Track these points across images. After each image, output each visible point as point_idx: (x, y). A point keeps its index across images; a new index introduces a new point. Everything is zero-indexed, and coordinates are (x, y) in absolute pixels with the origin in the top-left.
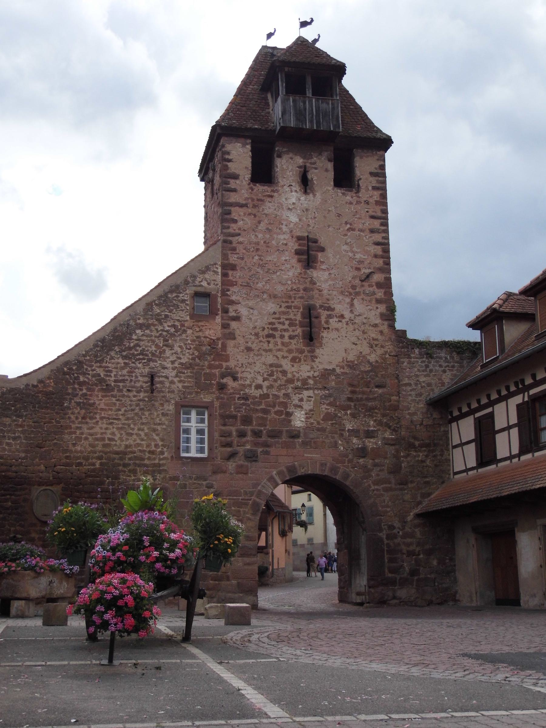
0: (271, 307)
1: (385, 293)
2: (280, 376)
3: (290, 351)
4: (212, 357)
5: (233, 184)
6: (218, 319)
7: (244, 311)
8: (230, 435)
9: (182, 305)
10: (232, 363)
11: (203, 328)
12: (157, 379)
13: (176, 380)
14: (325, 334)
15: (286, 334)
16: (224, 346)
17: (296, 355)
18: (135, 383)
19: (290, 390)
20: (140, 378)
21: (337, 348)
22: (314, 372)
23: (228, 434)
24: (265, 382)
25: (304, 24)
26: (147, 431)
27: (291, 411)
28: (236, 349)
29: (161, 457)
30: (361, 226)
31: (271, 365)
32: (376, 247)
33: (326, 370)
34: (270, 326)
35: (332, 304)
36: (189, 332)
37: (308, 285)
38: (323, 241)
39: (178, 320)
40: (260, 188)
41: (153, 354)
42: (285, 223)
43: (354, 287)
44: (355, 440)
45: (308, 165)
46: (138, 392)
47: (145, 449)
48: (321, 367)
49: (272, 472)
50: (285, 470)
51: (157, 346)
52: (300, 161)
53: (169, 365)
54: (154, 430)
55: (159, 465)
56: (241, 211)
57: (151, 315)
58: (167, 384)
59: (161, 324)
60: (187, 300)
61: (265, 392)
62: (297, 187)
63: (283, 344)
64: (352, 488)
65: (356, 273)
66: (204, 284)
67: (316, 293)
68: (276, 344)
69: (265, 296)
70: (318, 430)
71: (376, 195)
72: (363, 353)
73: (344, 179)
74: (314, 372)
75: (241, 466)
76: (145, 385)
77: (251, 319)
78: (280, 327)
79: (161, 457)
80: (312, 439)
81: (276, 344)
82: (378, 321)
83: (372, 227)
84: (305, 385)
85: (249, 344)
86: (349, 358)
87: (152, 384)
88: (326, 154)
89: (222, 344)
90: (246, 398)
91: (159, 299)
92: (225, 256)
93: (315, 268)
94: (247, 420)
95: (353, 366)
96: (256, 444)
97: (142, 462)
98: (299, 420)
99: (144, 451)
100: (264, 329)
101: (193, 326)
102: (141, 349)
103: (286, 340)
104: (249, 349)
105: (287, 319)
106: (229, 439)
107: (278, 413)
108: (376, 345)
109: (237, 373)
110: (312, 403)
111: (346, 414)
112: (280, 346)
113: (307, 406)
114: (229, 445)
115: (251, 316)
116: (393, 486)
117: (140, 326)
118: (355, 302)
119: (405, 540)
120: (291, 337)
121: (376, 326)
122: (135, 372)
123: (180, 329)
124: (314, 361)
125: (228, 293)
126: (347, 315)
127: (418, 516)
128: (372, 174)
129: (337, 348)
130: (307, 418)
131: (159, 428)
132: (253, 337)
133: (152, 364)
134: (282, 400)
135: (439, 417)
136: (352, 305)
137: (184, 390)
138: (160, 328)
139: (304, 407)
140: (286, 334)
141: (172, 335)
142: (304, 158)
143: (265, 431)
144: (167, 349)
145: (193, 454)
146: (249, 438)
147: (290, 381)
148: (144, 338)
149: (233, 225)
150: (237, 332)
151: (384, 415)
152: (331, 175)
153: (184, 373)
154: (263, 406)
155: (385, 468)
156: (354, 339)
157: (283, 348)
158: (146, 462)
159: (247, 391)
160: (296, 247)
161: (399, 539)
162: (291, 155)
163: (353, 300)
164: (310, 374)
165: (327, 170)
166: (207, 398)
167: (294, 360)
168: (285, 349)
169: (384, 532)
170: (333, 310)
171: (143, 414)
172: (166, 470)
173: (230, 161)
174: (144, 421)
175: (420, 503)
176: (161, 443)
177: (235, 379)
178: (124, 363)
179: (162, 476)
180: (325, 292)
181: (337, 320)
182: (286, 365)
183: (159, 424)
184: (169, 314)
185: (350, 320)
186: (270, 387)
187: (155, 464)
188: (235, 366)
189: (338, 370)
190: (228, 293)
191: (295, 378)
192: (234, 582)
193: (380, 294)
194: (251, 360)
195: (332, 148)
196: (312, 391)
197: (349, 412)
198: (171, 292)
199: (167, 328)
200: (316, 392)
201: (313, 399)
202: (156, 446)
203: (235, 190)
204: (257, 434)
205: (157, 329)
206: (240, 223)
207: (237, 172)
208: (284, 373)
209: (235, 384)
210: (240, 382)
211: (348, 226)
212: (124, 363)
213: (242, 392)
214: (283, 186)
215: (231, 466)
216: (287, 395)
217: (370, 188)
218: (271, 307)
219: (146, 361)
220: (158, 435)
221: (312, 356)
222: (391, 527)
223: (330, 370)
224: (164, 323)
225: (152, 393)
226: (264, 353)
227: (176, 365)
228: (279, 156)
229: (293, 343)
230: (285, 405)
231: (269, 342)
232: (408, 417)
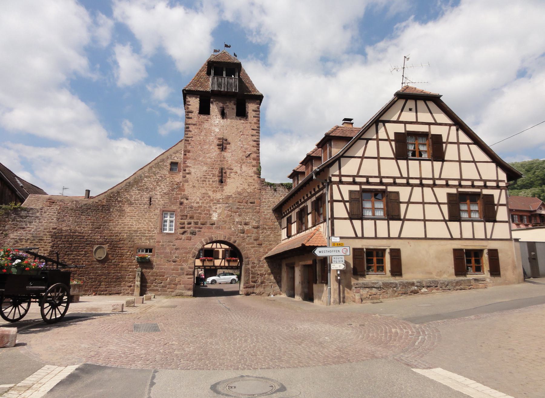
1: (257, 163)
5: (190, 115)
6: (181, 174)
7: (193, 171)
8: (184, 224)
10: (186, 193)
12: (152, 199)
13: (161, 200)
14: (228, 180)
16: (183, 185)
19: (211, 204)
25: (226, 46)
30: (247, 133)
31: (204, 194)
35: (232, 167)
36: (168, 179)
37: (222, 159)
38: (229, 140)
40: (202, 116)
41: (152, 189)
43: (242, 160)
44: (239, 226)
46: (144, 205)
48: (226, 194)
51: (153, 185)
53: (159, 193)
54: (151, 221)
55: (152, 236)
56: (194, 127)
62: (219, 116)
63: (209, 184)
65: (244, 154)
66: (176, 158)
67: (225, 163)
70: (223, 221)
71: (255, 120)
73: (242, 113)
78: (208, 177)
82: (253, 175)
83: (252, 134)
84: (218, 202)
85: (194, 184)
88: (233, 102)
92: (186, 147)
93: (225, 152)
96: (195, 228)
98: (215, 217)
103: (211, 182)
104: (194, 187)
106: (183, 226)
107: (205, 214)
112: (208, 185)
113: (219, 211)
114: (183, 228)
117: (146, 177)
118: (243, 166)
120: (213, 182)
121: (252, 176)
123: (163, 178)
126: (239, 172)
127: (266, 258)
128: (254, 111)
129: (233, 186)
131: (152, 220)
136: (241, 167)
138: (155, 177)
140: (211, 180)
145: (167, 231)
146: (192, 225)
149: (189, 133)
150: (189, 179)
151: (253, 215)
152: (235, 111)
154: (199, 211)
156: (241, 183)
158: (146, 235)
160: (218, 142)
165: (233, 109)
166: (174, 208)
167: (214, 191)
175: (267, 253)
177: (187, 199)
182: (210, 193)
186: (203, 203)
189: (233, 196)
193: (254, 163)
195: (236, 99)
198: (161, 162)
203: (191, 118)
204: (196, 223)
206: (193, 132)
207: (193, 110)
208: (209, 197)
215: (184, 237)
216: (210, 206)
218: (205, 168)
222: (253, 263)
225: (150, 205)
228: (212, 103)
230: (209, 211)
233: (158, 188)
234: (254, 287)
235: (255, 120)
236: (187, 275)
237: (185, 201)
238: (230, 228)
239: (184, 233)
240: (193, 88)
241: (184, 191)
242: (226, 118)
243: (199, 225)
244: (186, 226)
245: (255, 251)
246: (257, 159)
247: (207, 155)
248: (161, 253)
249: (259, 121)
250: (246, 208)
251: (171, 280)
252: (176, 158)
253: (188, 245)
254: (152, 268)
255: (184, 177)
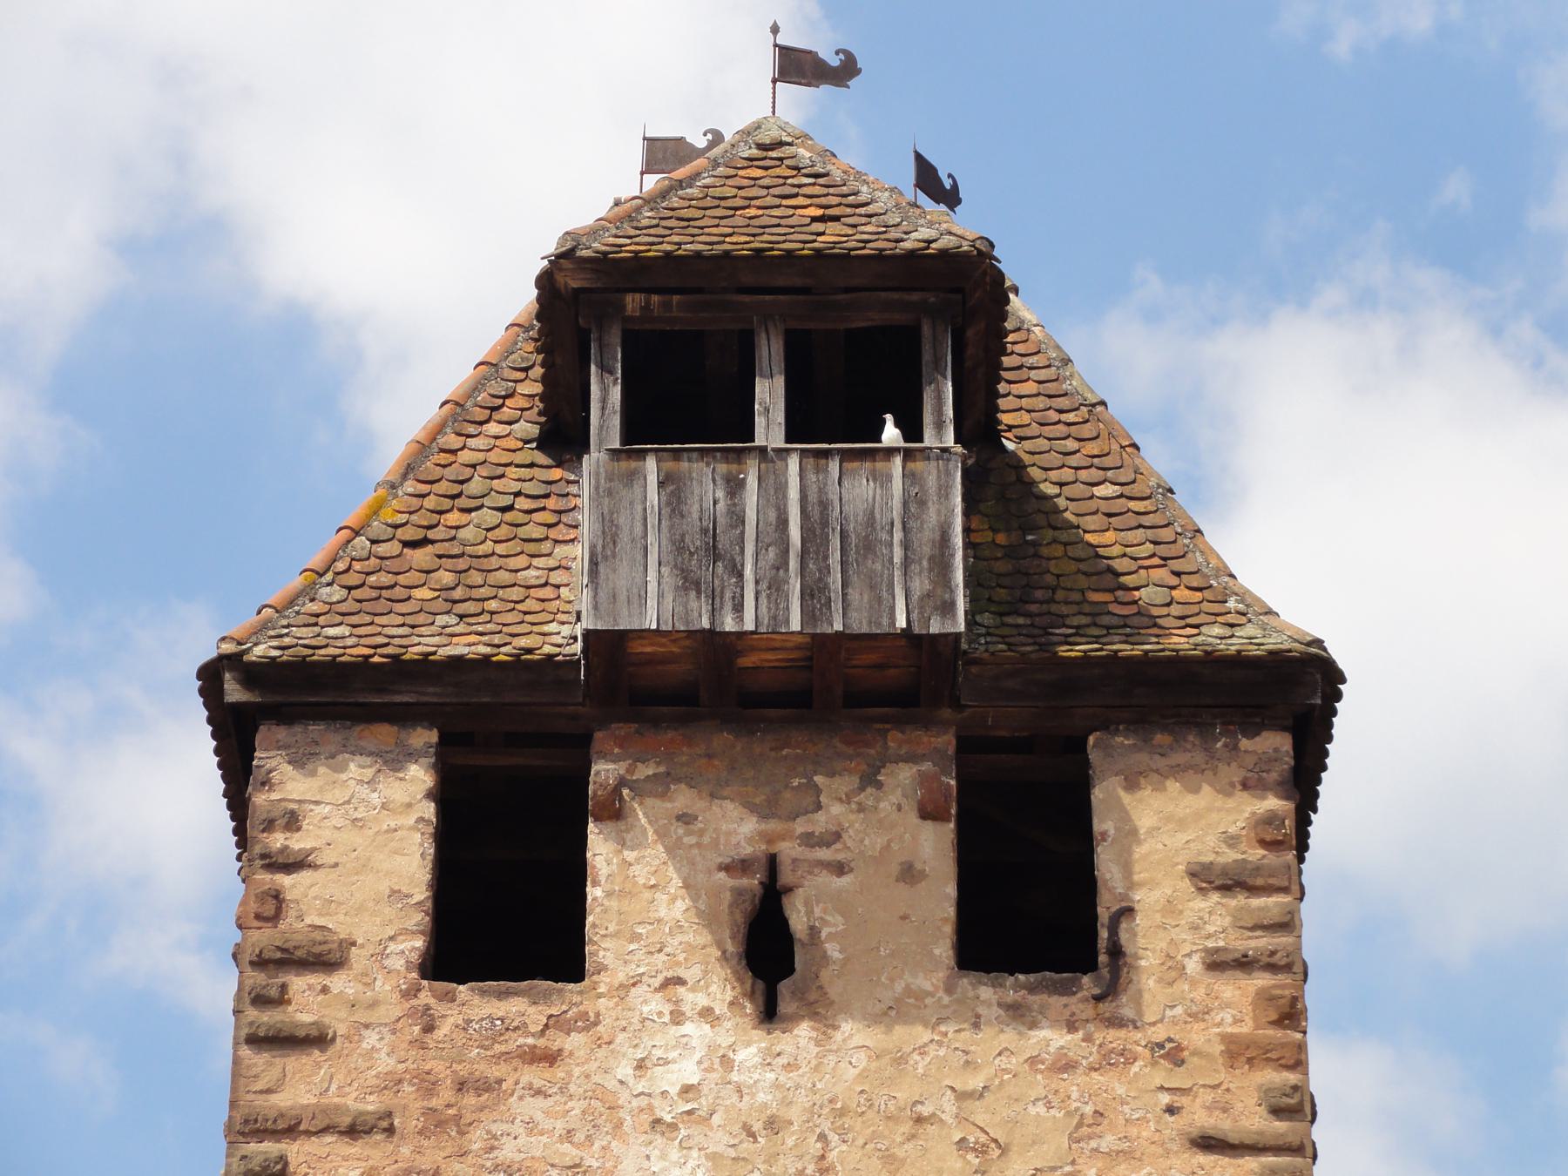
5: (308, 1002)
40: (475, 1005)
45: (788, 850)
52: (738, 828)
62: (717, 986)
71: (1236, 1004)
73: (1033, 916)
88: (902, 778)
128: (1209, 879)
142: (765, 811)
152: (940, 899)
162: (683, 798)
165: (909, 874)
195: (946, 741)
203: (317, 1040)
207: (339, 925)
214: (625, 988)
217: (1193, 965)
228: (613, 812)
235: (1236, 1004)
240: (342, 640)
242: (819, 1010)
249: (1291, 1015)
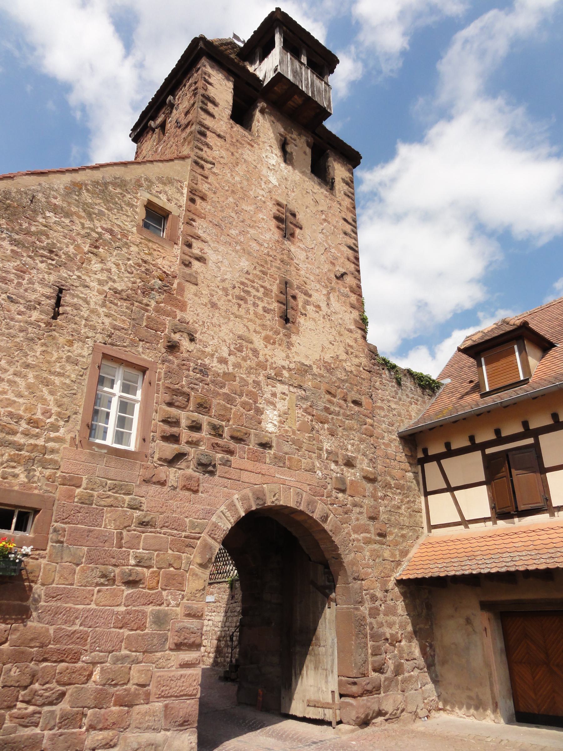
0: (245, 264)
2: (251, 355)
3: (263, 326)
4: (163, 297)
6: (177, 250)
7: (212, 256)
8: (177, 423)
9: (128, 208)
10: (189, 316)
11: (155, 253)
12: (67, 298)
13: (101, 310)
14: (301, 320)
15: (261, 305)
16: (181, 289)
17: (271, 333)
18: (26, 290)
19: (261, 378)
20: (37, 286)
21: (315, 341)
22: (290, 362)
23: (174, 420)
24: (232, 357)
26: (31, 380)
27: (261, 406)
28: (197, 298)
29: (52, 435)
31: (240, 337)
32: (349, 250)
33: (303, 364)
34: (242, 287)
36: (134, 249)
39: (119, 226)
41: (71, 258)
42: (264, 179)
44: (333, 466)
46: (29, 308)
47: (21, 413)
48: (297, 359)
49: (234, 494)
50: (251, 495)
51: (78, 247)
53: (94, 284)
54: (47, 383)
55: (45, 450)
56: (219, 142)
57: (76, 200)
58: (85, 313)
59: (91, 220)
60: (137, 207)
61: (231, 370)
63: (256, 313)
64: (331, 534)
65: (331, 267)
66: (164, 197)
68: (248, 311)
69: (238, 248)
70: (294, 442)
72: (340, 358)
74: (290, 362)
75: (190, 478)
76: (45, 301)
77: (219, 268)
78: (254, 292)
79: (52, 435)
80: (286, 453)
81: (248, 311)
82: (353, 327)
84: (277, 378)
85: (215, 299)
86: (326, 358)
87: (58, 304)
89: (179, 284)
90: (204, 370)
91: (94, 186)
92: (193, 180)
93: (293, 243)
94: (203, 407)
95: (330, 369)
96: (215, 446)
97: (11, 438)
98: (271, 422)
99: (20, 418)
100: (234, 287)
101: (140, 243)
102: (49, 241)
103: (260, 310)
104: (214, 305)
105: (262, 287)
106: (174, 430)
107: (244, 405)
108: (352, 353)
109: (196, 332)
110: (286, 402)
111: (323, 428)
112: (252, 316)
113: (282, 405)
114: (174, 439)
115: (219, 264)
116: (373, 537)
117: (55, 209)
119: (388, 618)
120: (265, 310)
121: (350, 331)
122: (30, 274)
123: (118, 239)
124: (290, 349)
125: (194, 223)
129: (315, 341)
130: (280, 422)
131: (57, 380)
132: (220, 293)
133: (64, 273)
134: (250, 388)
135: (410, 455)
136: (329, 299)
137: (113, 331)
138: (88, 224)
139: (279, 406)
140: (261, 305)
141: (106, 243)
142: (285, 129)
143: (226, 428)
144: (94, 259)
145: (109, 441)
146: (205, 433)
147: (262, 366)
148: (59, 228)
149: (205, 149)
150: (200, 278)
151: (361, 441)
153: (116, 305)
154: (225, 390)
155: (364, 510)
157: (256, 319)
158: (19, 439)
159: (207, 361)
161: (382, 616)
163: (329, 293)
164: (286, 363)
166: (145, 355)
167: (267, 339)
168: (258, 322)
169: (366, 605)
170: (310, 296)
171: (32, 349)
172: (56, 462)
173: (210, 84)
174: (30, 360)
176: (55, 409)
177: (192, 340)
178: (12, 251)
179: (47, 472)
180: (302, 272)
181: (314, 309)
182: (258, 342)
183: (59, 374)
184: (106, 211)
185: (327, 314)
186: (237, 366)
187: (36, 445)
188: (195, 322)
189: (315, 370)
190: (194, 223)
191: (268, 363)
192: (158, 705)
194: (215, 320)
196: (287, 387)
197: (326, 426)
198: (115, 185)
199: (99, 230)
200: (292, 389)
201: (288, 398)
202: (47, 413)
204: (217, 431)
205: (83, 224)
208: (255, 352)
209: (191, 347)
210: (198, 346)
211: (324, 217)
212: (12, 251)
213: (199, 361)
214: (264, 142)
215: (173, 475)
216: (257, 383)
218: (245, 264)
219: (54, 262)
220: (52, 393)
221: (288, 342)
222: (374, 598)
223: (306, 365)
224: (96, 221)
225: (55, 317)
226: (232, 317)
227: (106, 288)
229: (267, 318)
230: (254, 397)
231: (240, 306)
232: (383, 447)
233: (96, 266)
234: (377, 689)
235: (347, 202)
236: (178, 647)
237: (185, 344)
238: (312, 470)
239: (174, 461)
241: (183, 307)
243: (225, 441)
244: (185, 435)
245: (375, 555)
246: (357, 291)
247: (252, 231)
248: (77, 539)
250: (347, 417)
251: (110, 681)
252: (164, 197)
253: (186, 508)
254: (23, 614)
255: (187, 265)
